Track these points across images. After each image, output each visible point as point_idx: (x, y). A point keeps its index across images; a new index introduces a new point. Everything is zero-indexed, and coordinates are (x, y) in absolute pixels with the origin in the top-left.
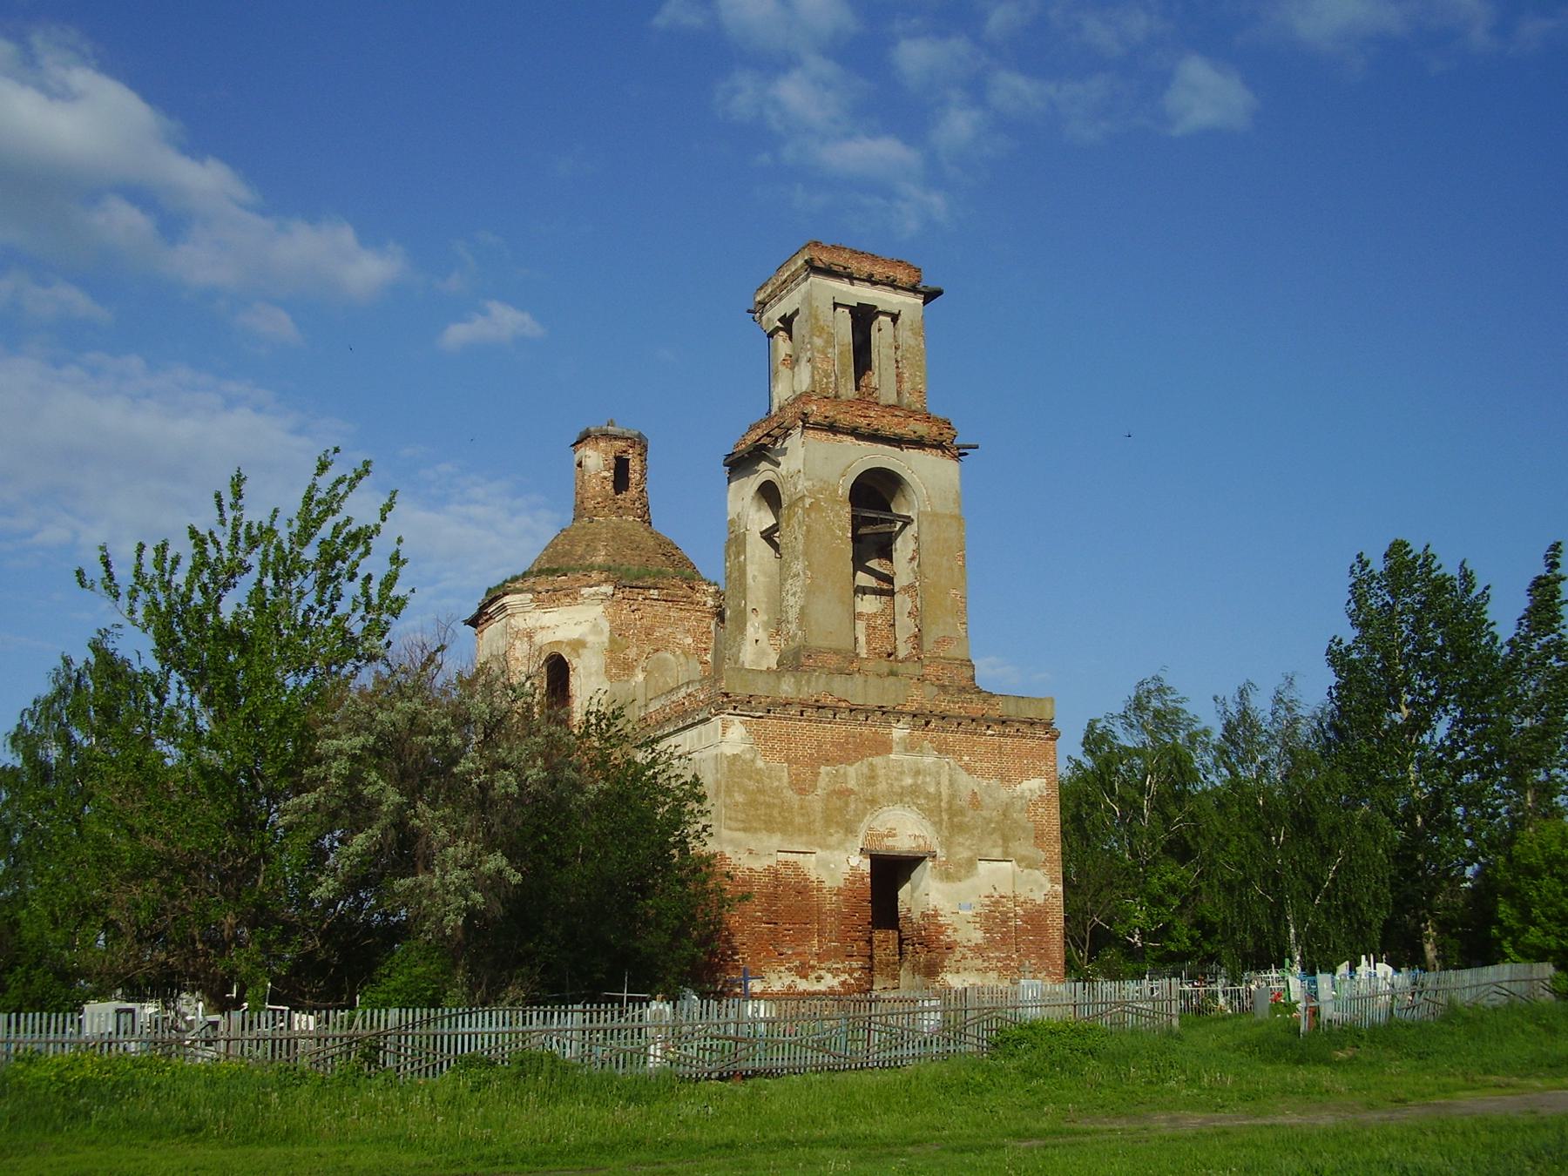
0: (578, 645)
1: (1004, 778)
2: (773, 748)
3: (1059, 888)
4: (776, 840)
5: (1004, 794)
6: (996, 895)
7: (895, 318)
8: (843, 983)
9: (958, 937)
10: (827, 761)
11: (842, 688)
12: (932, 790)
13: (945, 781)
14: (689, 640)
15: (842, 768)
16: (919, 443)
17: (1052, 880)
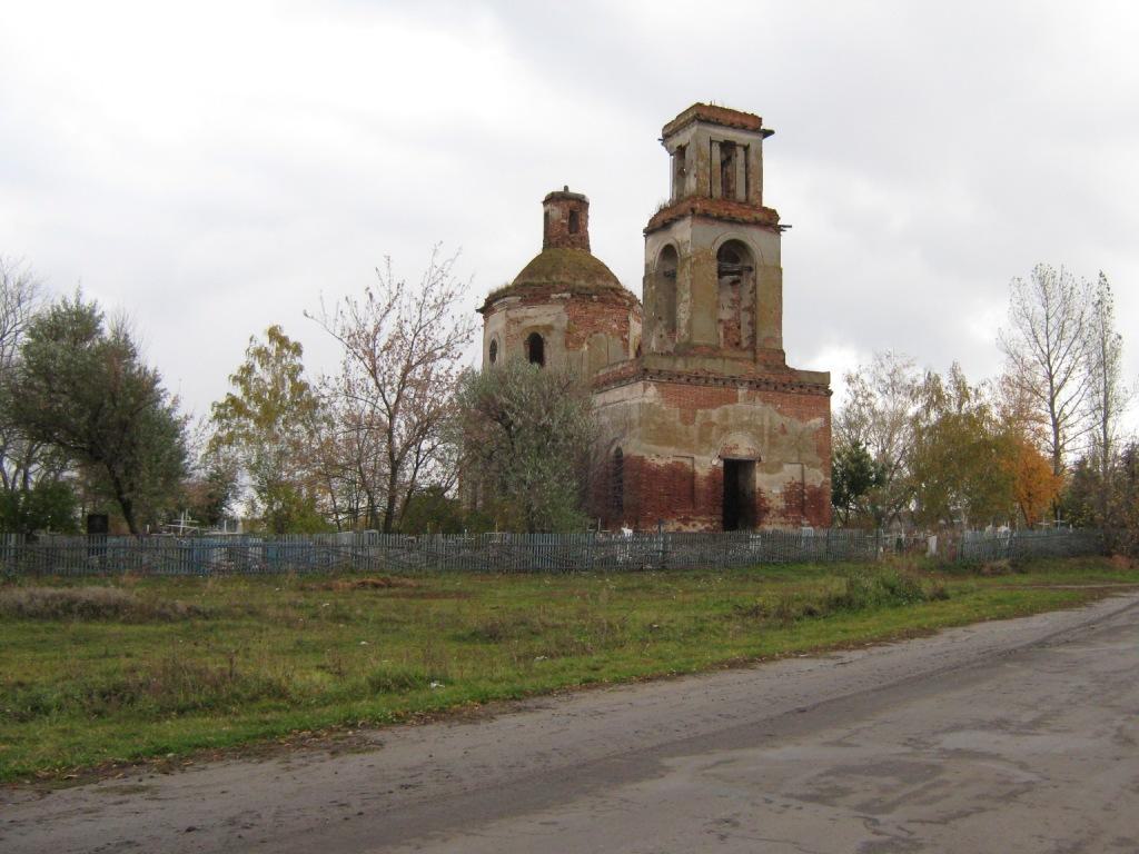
0: (549, 328)
1: (801, 418)
3: (829, 479)
4: (672, 450)
5: (800, 426)
7: (746, 148)
8: (707, 529)
9: (771, 505)
10: (702, 407)
11: (711, 365)
12: (759, 423)
13: (766, 419)
14: (615, 326)
15: (709, 410)
16: (757, 223)
17: (826, 475)
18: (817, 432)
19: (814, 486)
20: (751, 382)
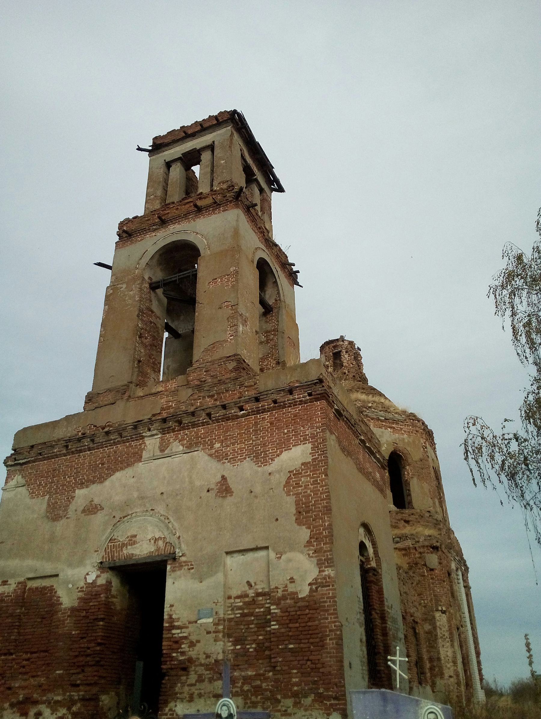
1: (261, 457)
2: (40, 484)
9: (193, 653)
10: (82, 485)
18: (295, 474)
19: (294, 595)
20: (164, 420)
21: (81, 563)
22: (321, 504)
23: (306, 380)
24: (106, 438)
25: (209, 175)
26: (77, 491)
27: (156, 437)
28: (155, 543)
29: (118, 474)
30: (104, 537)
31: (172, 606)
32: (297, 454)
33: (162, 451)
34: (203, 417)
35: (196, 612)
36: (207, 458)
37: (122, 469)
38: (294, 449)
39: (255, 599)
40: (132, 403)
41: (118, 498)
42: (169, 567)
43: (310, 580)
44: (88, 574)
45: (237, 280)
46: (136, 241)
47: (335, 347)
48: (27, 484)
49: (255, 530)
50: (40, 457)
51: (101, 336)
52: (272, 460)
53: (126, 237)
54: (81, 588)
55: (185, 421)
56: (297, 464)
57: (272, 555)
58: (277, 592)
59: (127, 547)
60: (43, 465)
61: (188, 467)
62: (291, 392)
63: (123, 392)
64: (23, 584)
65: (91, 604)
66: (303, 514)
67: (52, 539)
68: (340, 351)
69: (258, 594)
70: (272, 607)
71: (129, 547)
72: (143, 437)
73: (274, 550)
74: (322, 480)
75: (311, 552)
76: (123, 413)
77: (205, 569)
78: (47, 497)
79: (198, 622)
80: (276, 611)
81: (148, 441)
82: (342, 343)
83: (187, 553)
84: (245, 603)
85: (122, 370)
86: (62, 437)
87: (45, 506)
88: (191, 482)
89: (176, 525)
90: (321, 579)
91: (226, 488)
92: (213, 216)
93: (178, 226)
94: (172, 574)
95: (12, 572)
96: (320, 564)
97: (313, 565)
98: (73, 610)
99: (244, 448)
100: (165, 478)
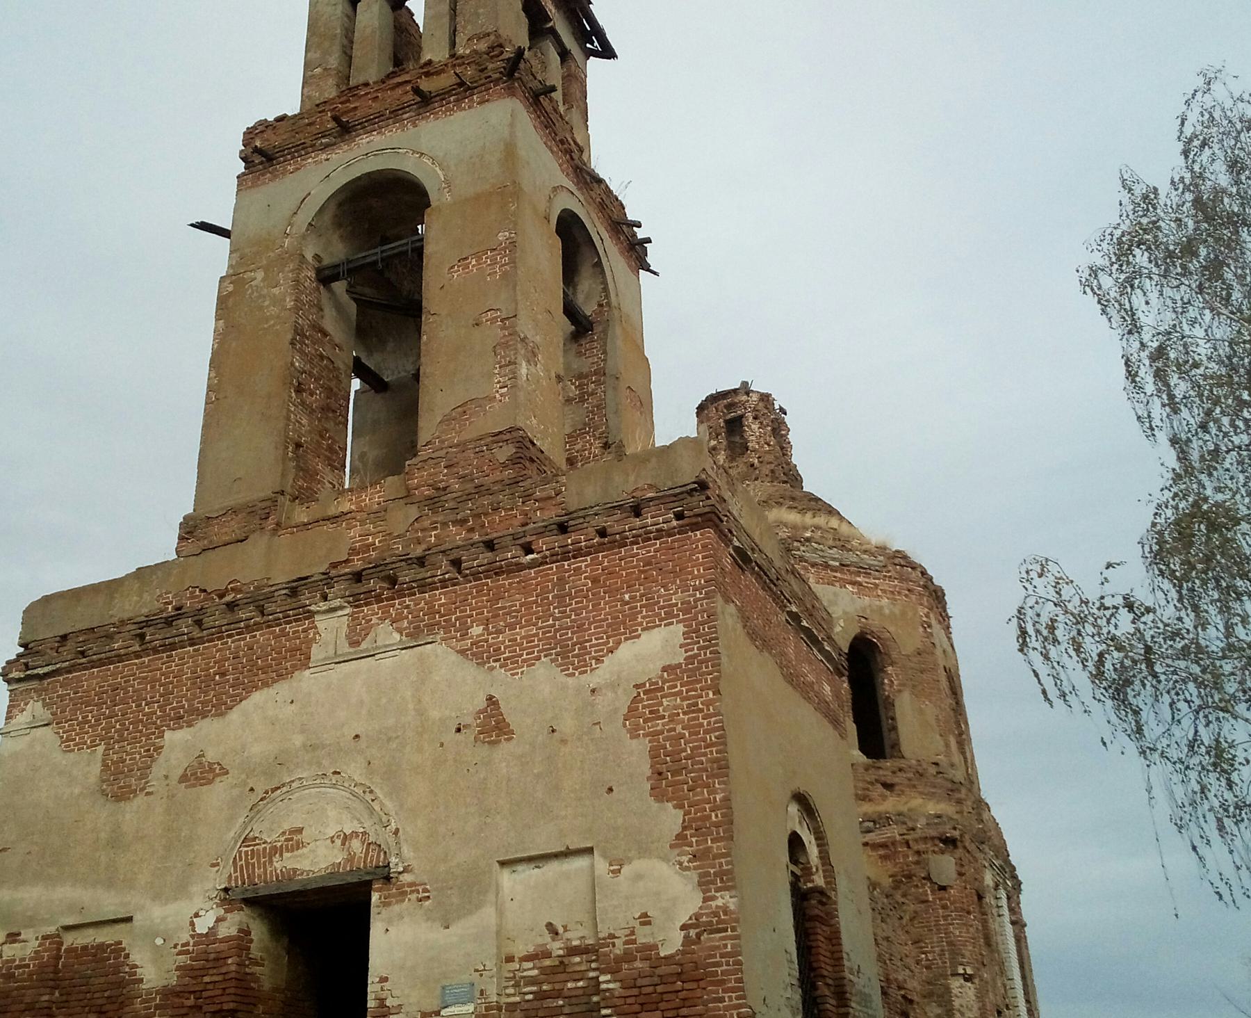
1: (572, 654)
2: (85, 721)
6: (557, 948)
10: (179, 720)
18: (651, 690)
20: (358, 577)
21: (181, 890)
22: (705, 755)
23: (670, 484)
24: (230, 617)
25: (446, 20)
26: (168, 734)
27: (340, 613)
28: (343, 844)
29: (257, 697)
30: (232, 834)
31: (384, 980)
32: (653, 648)
33: (355, 643)
34: (443, 568)
35: (438, 992)
36: (454, 657)
37: (266, 685)
38: (645, 636)
39: (566, 960)
40: (284, 539)
41: (257, 751)
42: (375, 897)
43: (684, 919)
44: (197, 915)
45: (513, 262)
46: (284, 173)
47: (730, 407)
48: (55, 721)
49: (563, 813)
50: (84, 660)
51: (210, 388)
52: (598, 661)
53: (261, 163)
54: (183, 945)
55: (406, 576)
56: (653, 670)
57: (601, 866)
58: (614, 945)
59: (281, 855)
60: (91, 680)
61: (413, 678)
62: (637, 511)
63: (262, 515)
64: (54, 940)
65: (207, 979)
66: (667, 777)
67: (116, 841)
68: (742, 416)
69: (572, 951)
70: (602, 979)
71: (286, 855)
72: (311, 614)
73: (604, 856)
74: (708, 704)
75: (685, 859)
76: (262, 562)
77: (455, 900)
78: (101, 749)
79: (443, 1013)
80: (611, 986)
81: (322, 623)
82: (744, 398)
83: (414, 864)
84: (543, 970)
85: (260, 465)
86: (131, 615)
87: (97, 768)
88: (421, 713)
89: (390, 805)
90: (707, 915)
91: (497, 723)
92: (459, 115)
93: (379, 137)
94: (384, 912)
95: (29, 913)
96: (704, 884)
97: (690, 887)
98: (168, 993)
99: (536, 635)
100: (362, 702)
